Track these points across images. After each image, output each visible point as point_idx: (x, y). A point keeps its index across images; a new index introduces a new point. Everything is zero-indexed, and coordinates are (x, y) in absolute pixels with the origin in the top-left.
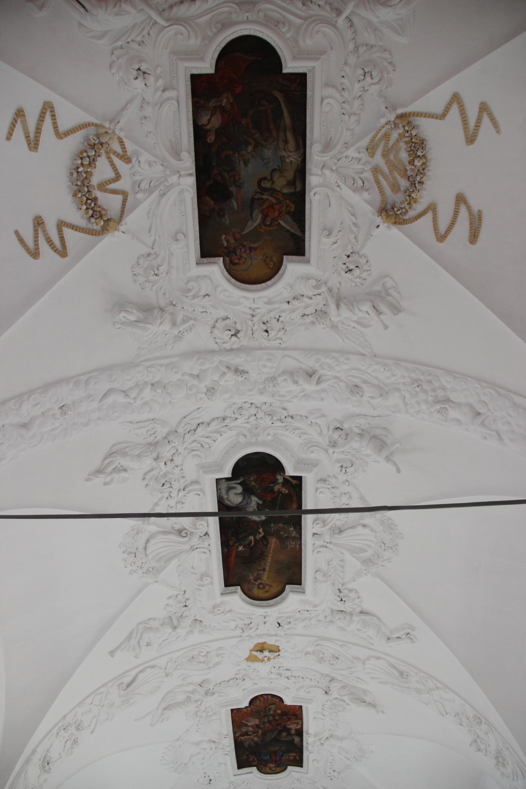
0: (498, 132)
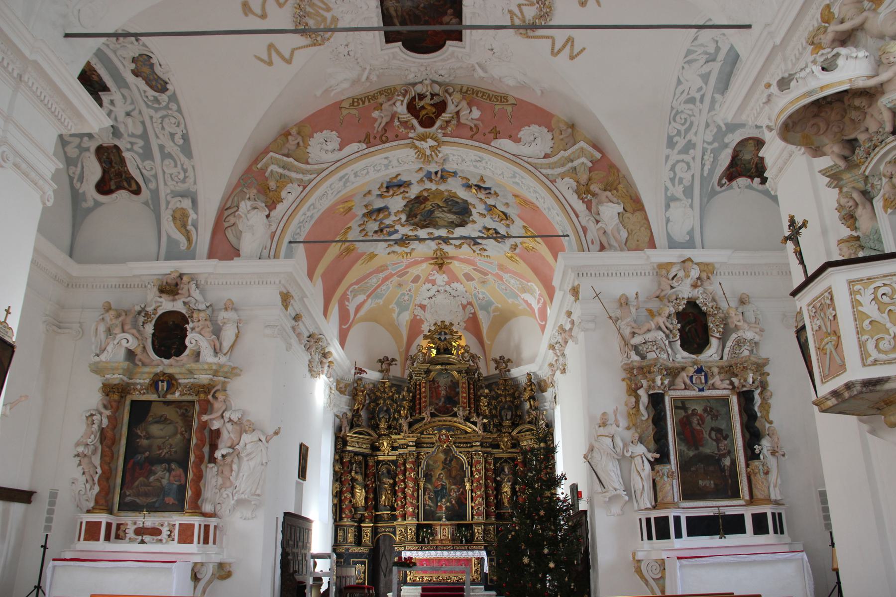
0: (256, 56)
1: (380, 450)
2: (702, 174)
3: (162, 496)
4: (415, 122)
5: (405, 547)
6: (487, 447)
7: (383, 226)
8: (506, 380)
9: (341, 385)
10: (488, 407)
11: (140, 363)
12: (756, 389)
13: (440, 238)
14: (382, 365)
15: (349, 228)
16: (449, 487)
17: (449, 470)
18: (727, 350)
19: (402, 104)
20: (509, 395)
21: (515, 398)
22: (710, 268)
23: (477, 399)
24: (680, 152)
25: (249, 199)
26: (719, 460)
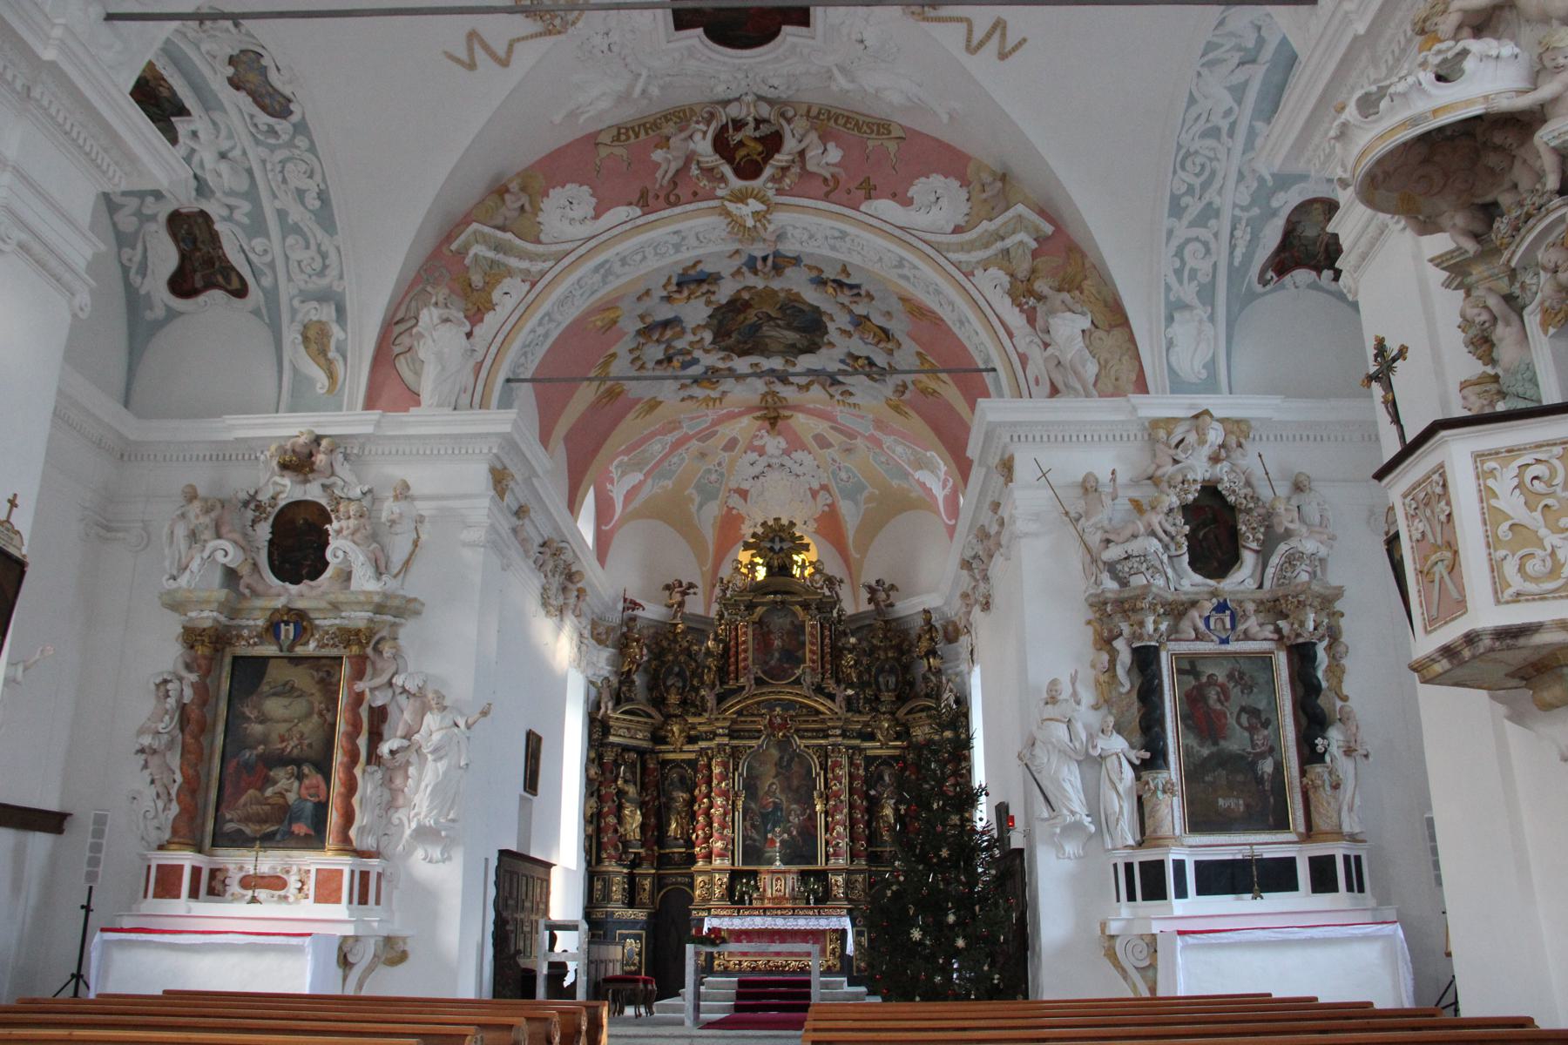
1: (666, 743)
2: (1231, 264)
3: (286, 822)
4: (727, 170)
5: (709, 909)
6: (854, 738)
7: (671, 351)
8: (886, 622)
9: (601, 630)
11: (247, 592)
12: (1321, 639)
13: (772, 371)
15: (614, 355)
18: (1270, 571)
19: (704, 138)
20: (892, 647)
22: (1244, 427)
23: (837, 653)
24: (1192, 225)
25: (436, 304)
26: (1253, 765)
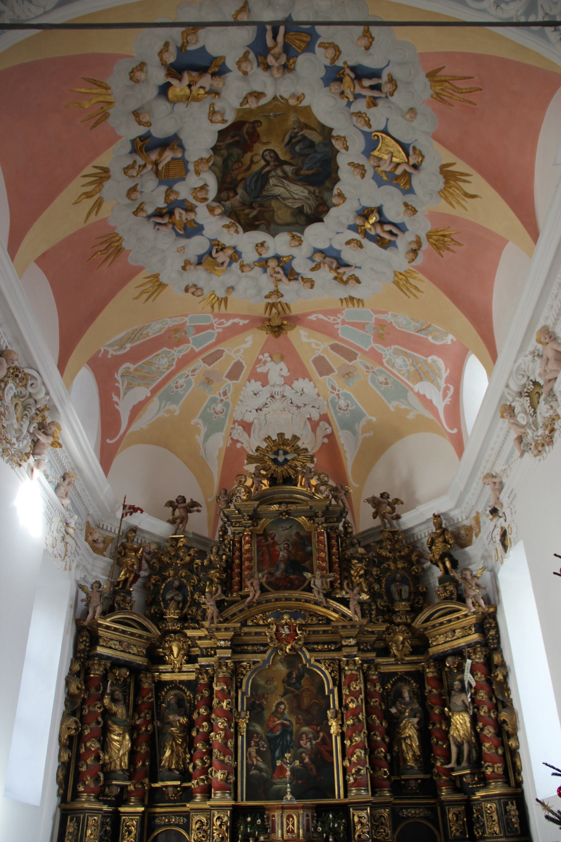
1: (165, 663)
6: (368, 651)
8: (394, 533)
9: (96, 536)
10: (366, 579)
14: (174, 510)
16: (298, 731)
17: (296, 696)
20: (401, 558)
21: (411, 564)
